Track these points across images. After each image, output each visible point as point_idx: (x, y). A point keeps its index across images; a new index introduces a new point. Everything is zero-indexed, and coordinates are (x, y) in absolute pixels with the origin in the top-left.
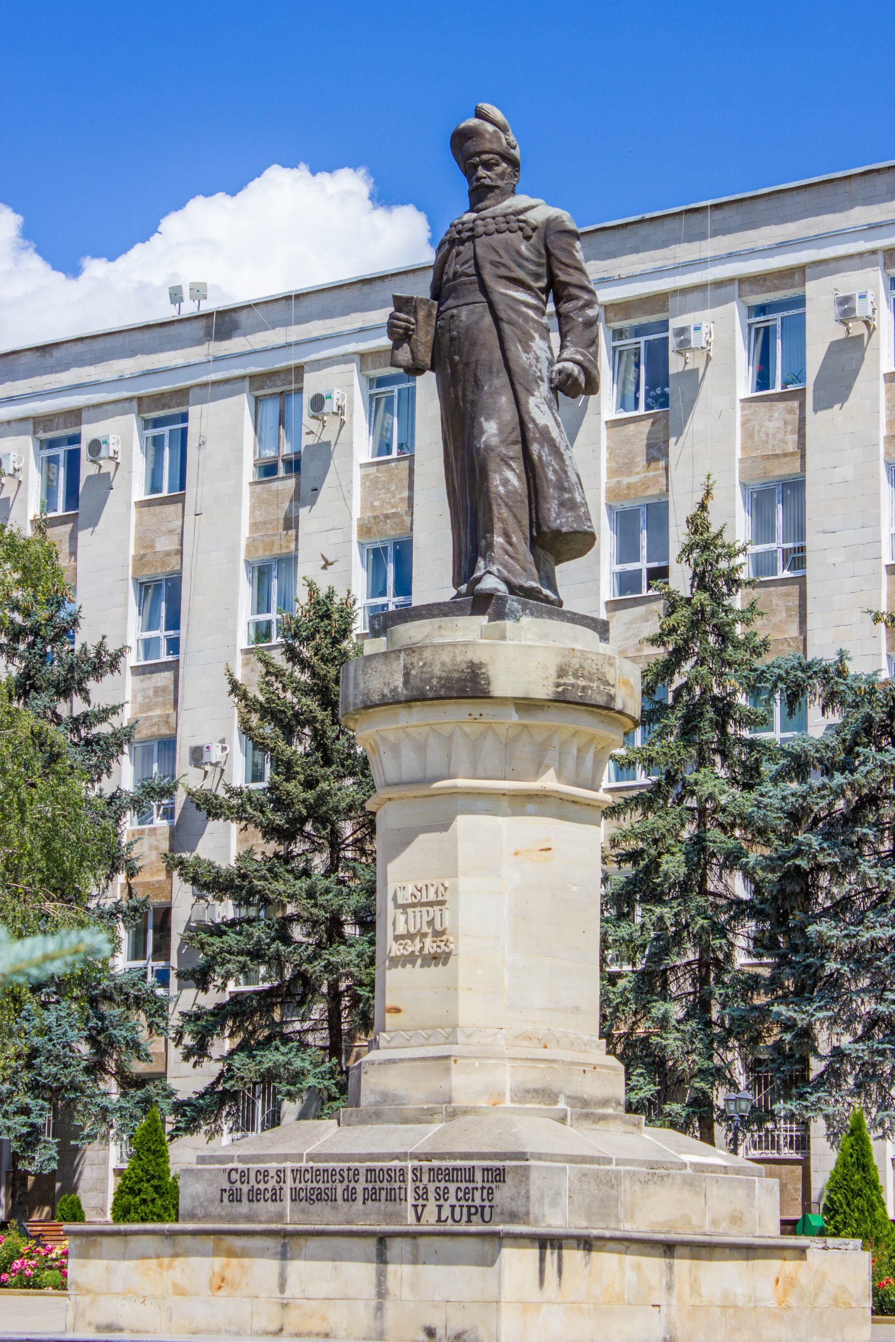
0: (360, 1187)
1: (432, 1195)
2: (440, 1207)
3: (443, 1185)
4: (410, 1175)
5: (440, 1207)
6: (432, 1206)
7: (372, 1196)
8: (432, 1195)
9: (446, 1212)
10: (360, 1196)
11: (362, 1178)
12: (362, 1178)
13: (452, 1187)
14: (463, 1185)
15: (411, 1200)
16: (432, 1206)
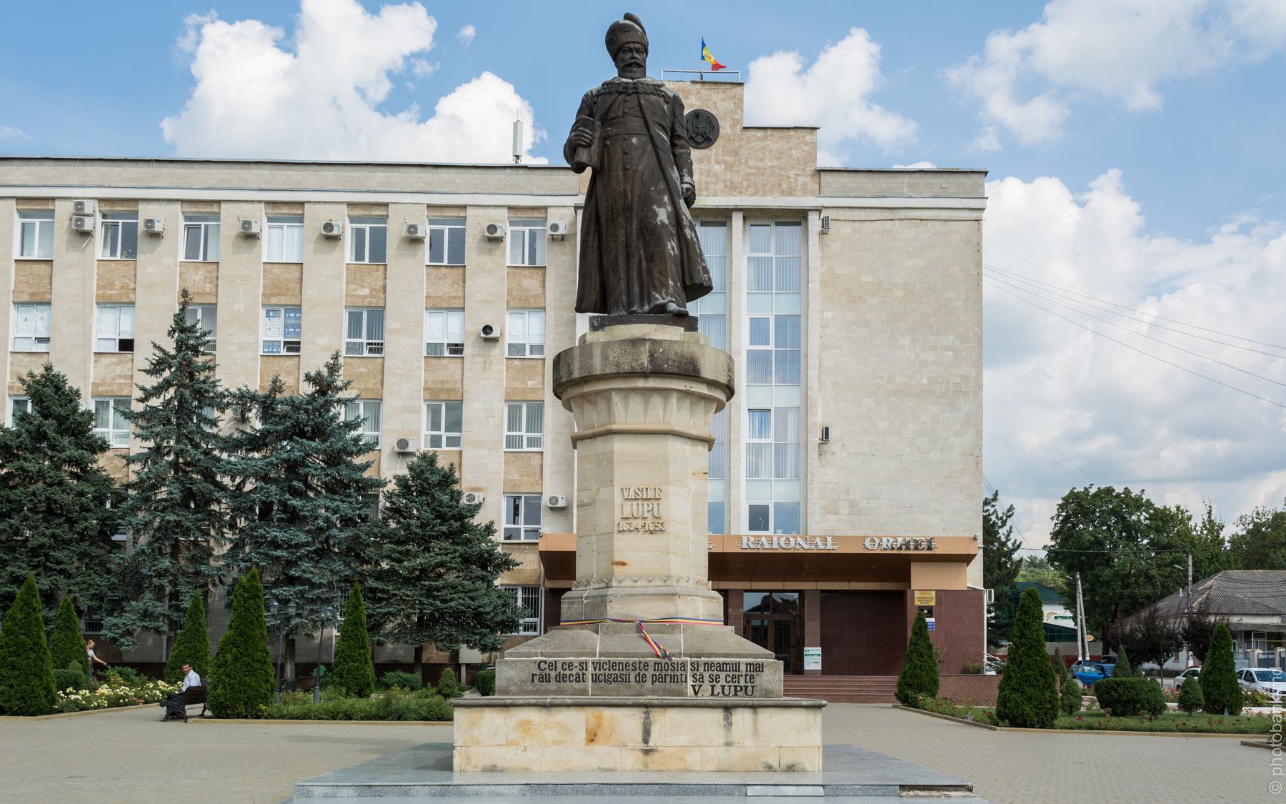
0: (649, 674)
1: (706, 678)
2: (713, 687)
3: (715, 673)
4: (689, 667)
5: (713, 687)
6: (707, 685)
7: (661, 679)
8: (706, 678)
9: (718, 689)
10: (649, 679)
11: (651, 669)
12: (651, 669)
13: (723, 675)
14: (731, 674)
15: (690, 682)
16: (707, 685)
